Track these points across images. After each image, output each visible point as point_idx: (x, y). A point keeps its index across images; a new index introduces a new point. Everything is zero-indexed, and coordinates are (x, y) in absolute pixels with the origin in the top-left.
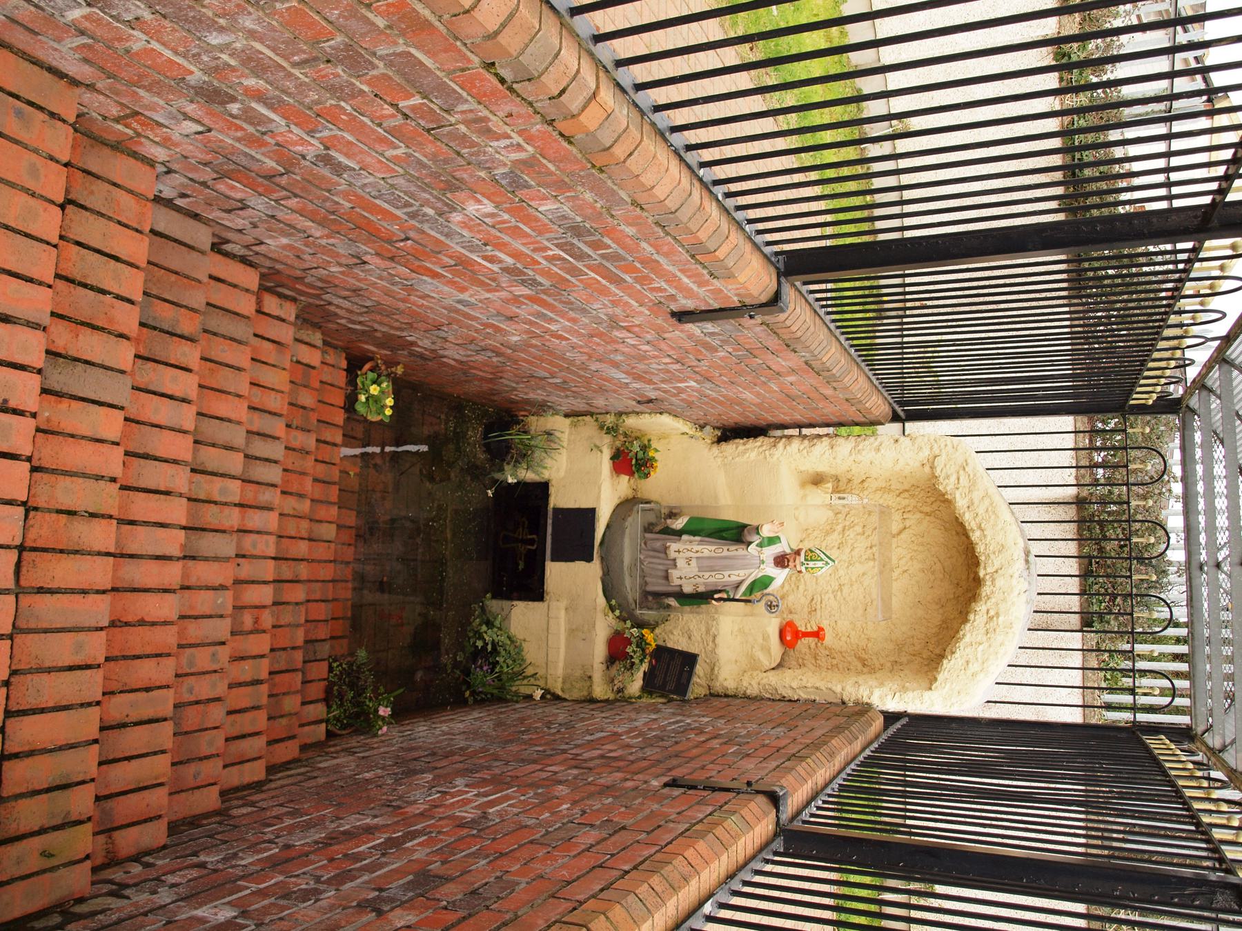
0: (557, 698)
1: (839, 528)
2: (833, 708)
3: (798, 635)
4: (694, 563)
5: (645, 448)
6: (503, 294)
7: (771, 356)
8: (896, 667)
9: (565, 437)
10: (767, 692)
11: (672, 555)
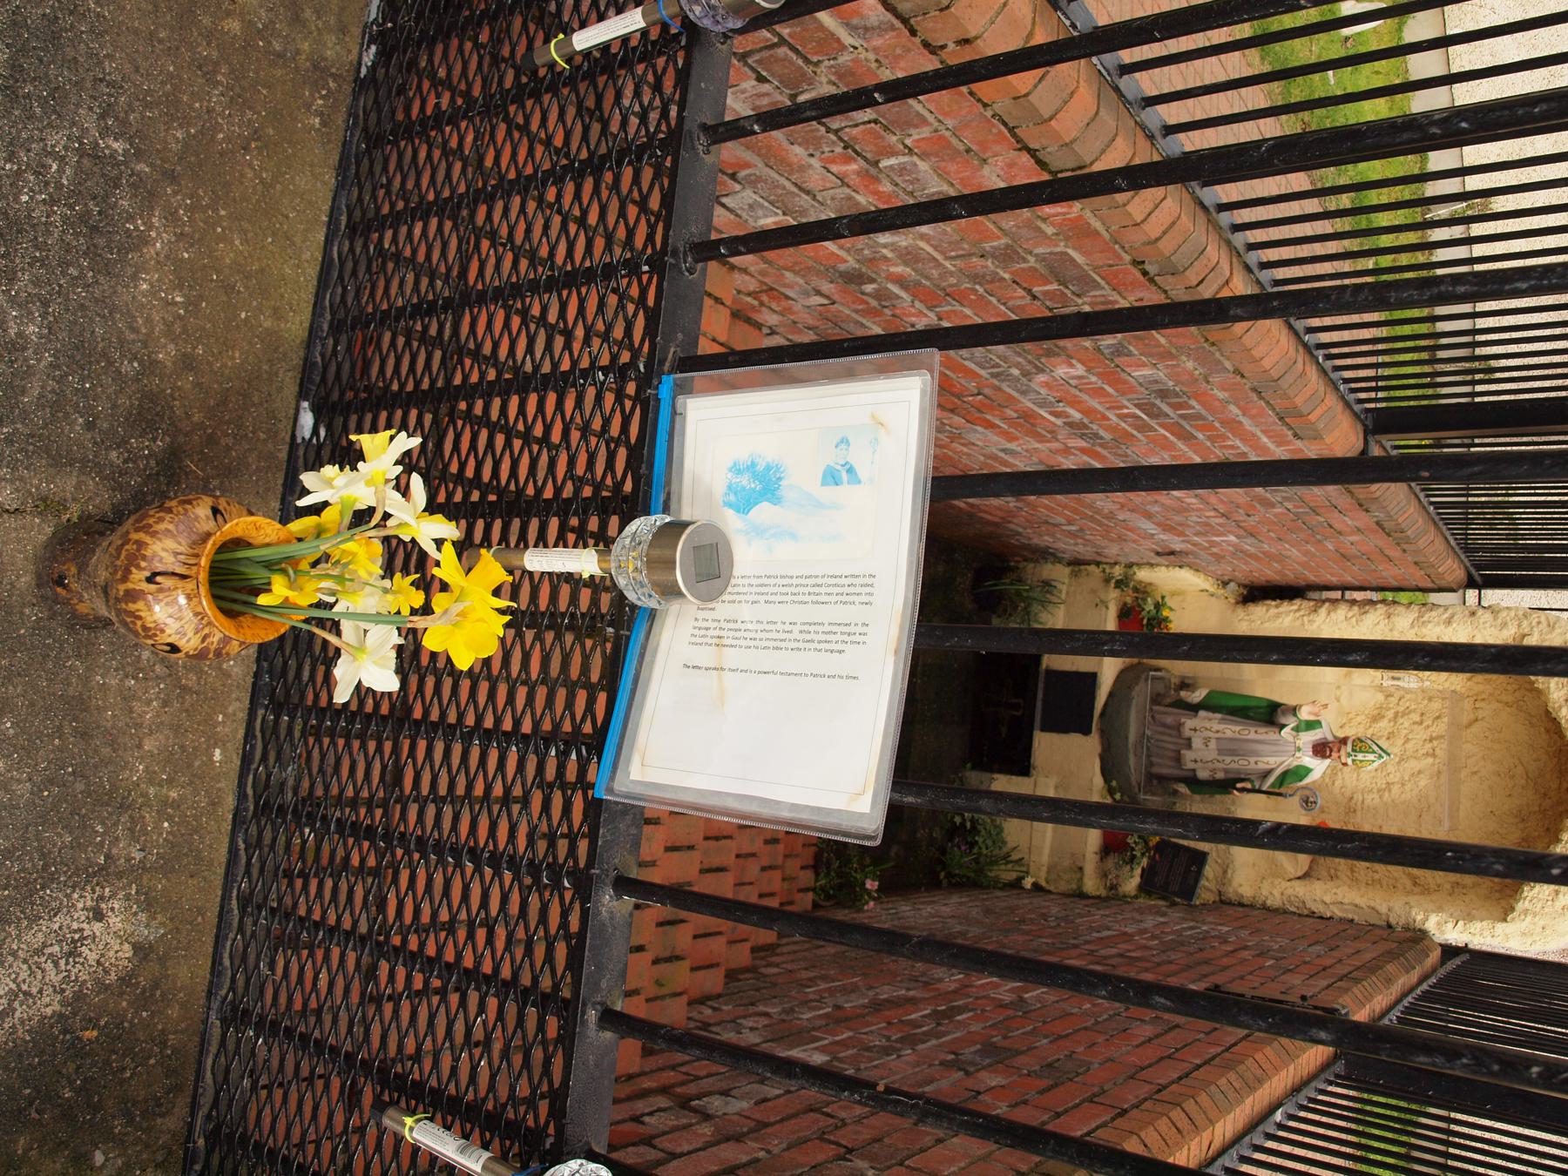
1: (1390, 714)
2: (1377, 931)
4: (1213, 745)
5: (1158, 606)
6: (1056, 445)
7: (1337, 514)
9: (1064, 588)
10: (1291, 904)
11: (1187, 733)
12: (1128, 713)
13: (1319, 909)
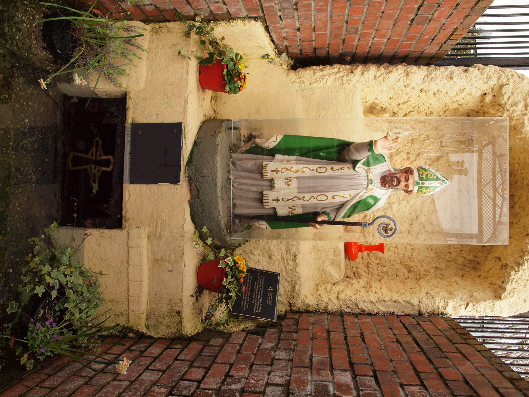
0: (140, 337)
3: (360, 248)
4: (294, 184)
8: (440, 273)
11: (269, 174)
12: (214, 157)
13: (367, 307)
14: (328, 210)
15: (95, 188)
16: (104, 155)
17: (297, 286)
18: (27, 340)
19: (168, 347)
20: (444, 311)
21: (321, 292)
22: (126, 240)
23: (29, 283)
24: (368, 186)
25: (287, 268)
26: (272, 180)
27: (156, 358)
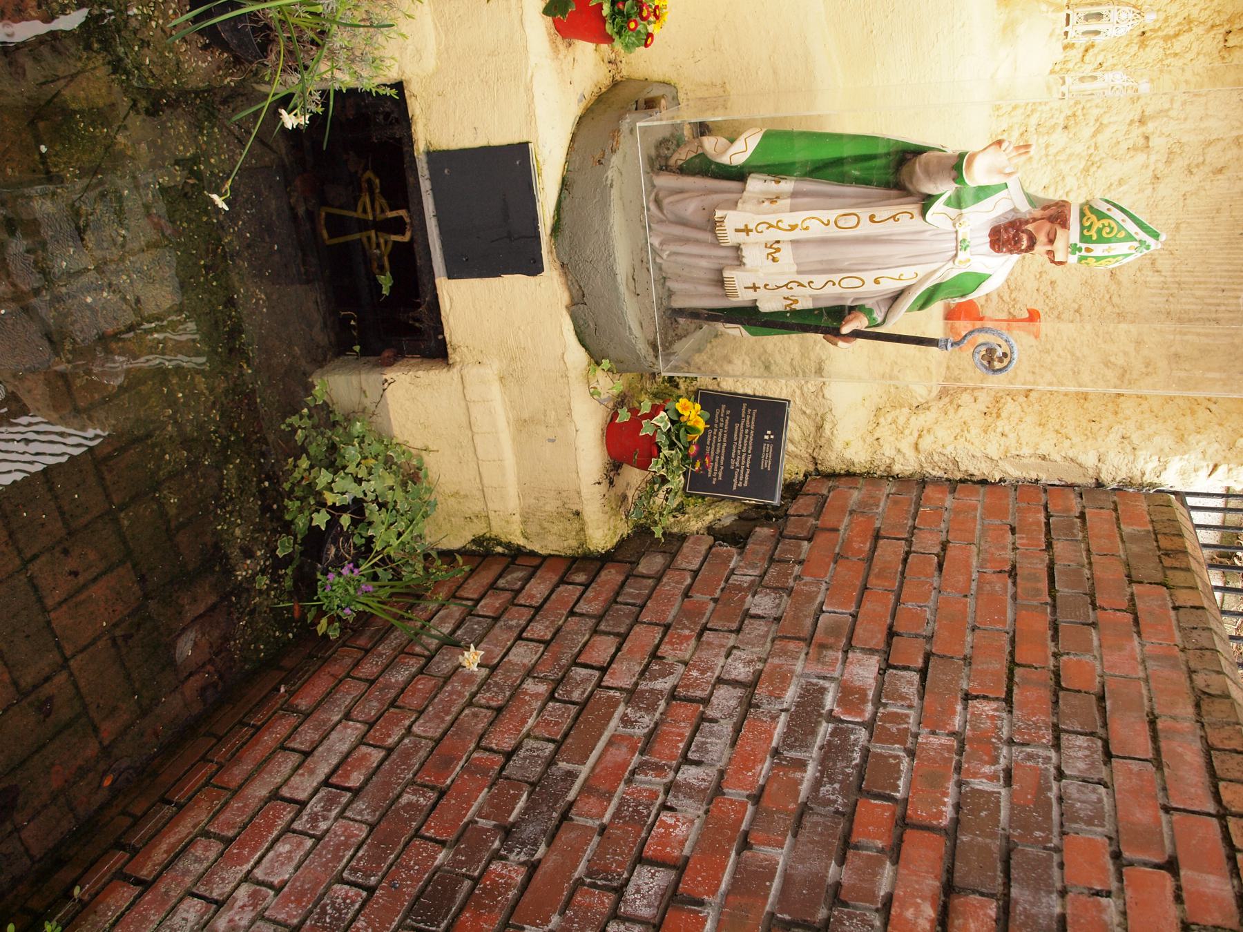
0: (516, 555)
11: (732, 238)
12: (605, 217)
13: (979, 469)
14: (869, 304)
15: (386, 282)
16: (391, 210)
17: (827, 426)
18: (319, 600)
19: (562, 581)
20: (1156, 480)
21: (884, 432)
22: (460, 387)
23: (301, 510)
24: (956, 255)
25: (805, 389)
26: (738, 248)
27: (538, 609)
